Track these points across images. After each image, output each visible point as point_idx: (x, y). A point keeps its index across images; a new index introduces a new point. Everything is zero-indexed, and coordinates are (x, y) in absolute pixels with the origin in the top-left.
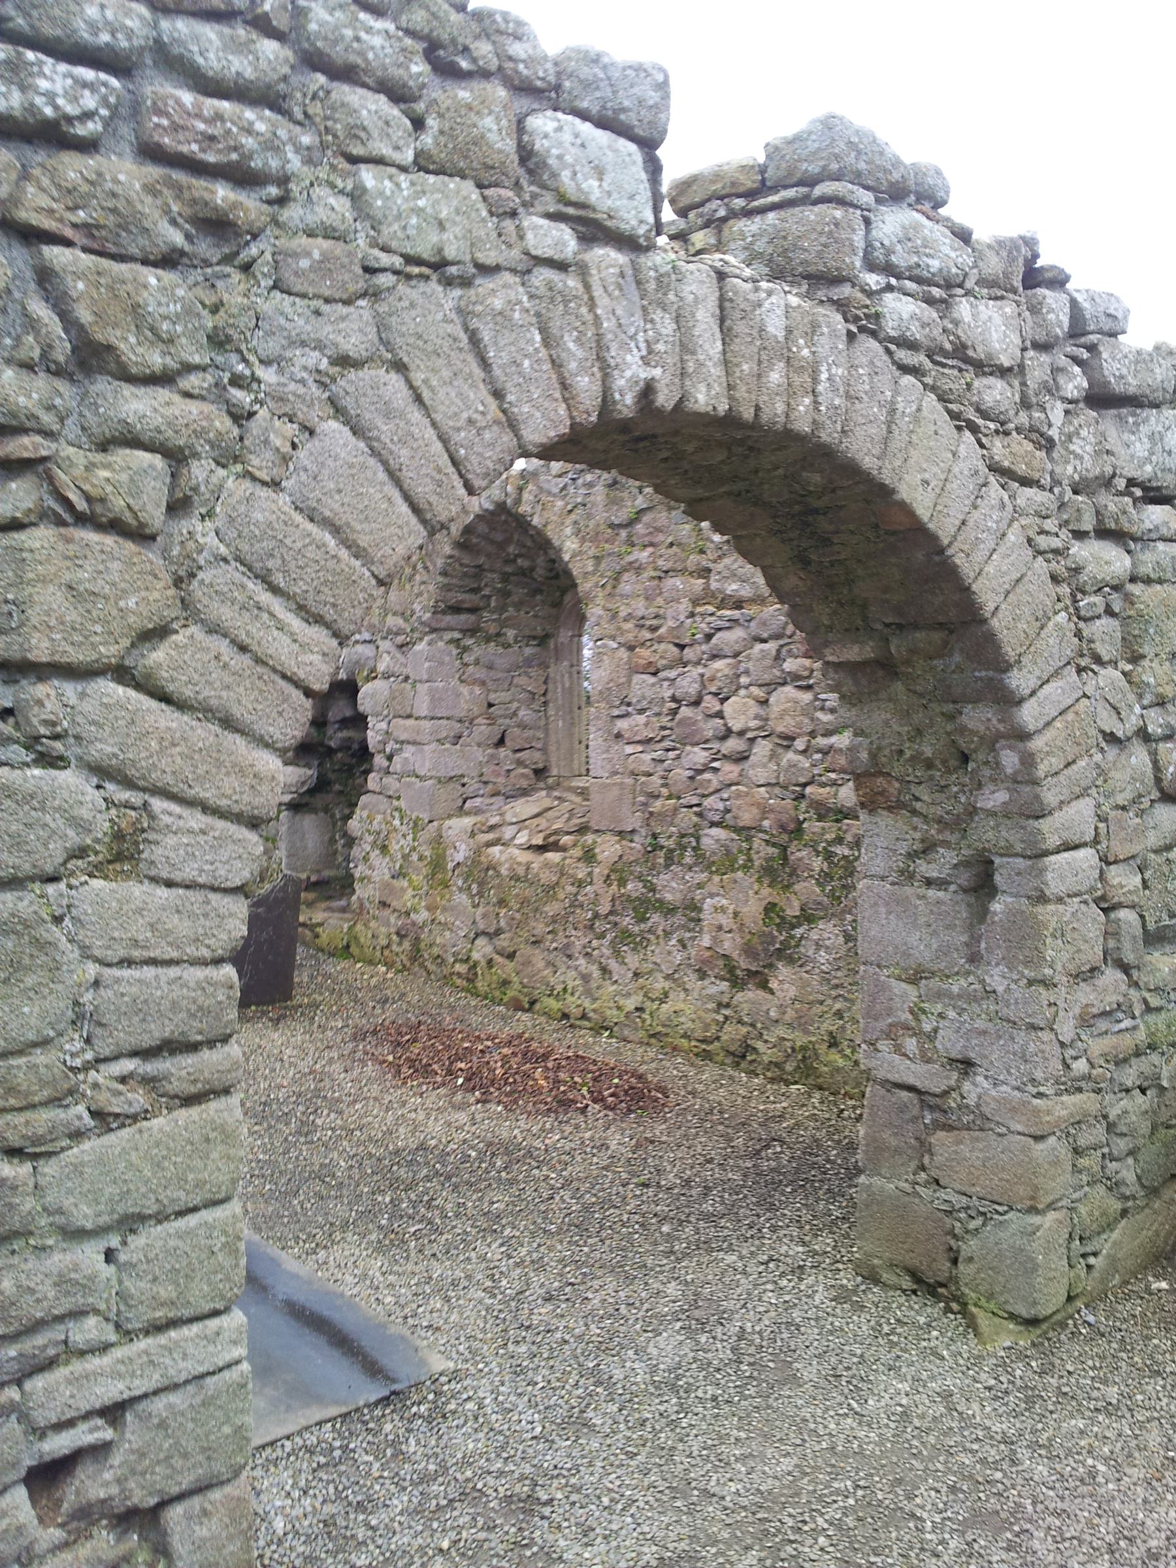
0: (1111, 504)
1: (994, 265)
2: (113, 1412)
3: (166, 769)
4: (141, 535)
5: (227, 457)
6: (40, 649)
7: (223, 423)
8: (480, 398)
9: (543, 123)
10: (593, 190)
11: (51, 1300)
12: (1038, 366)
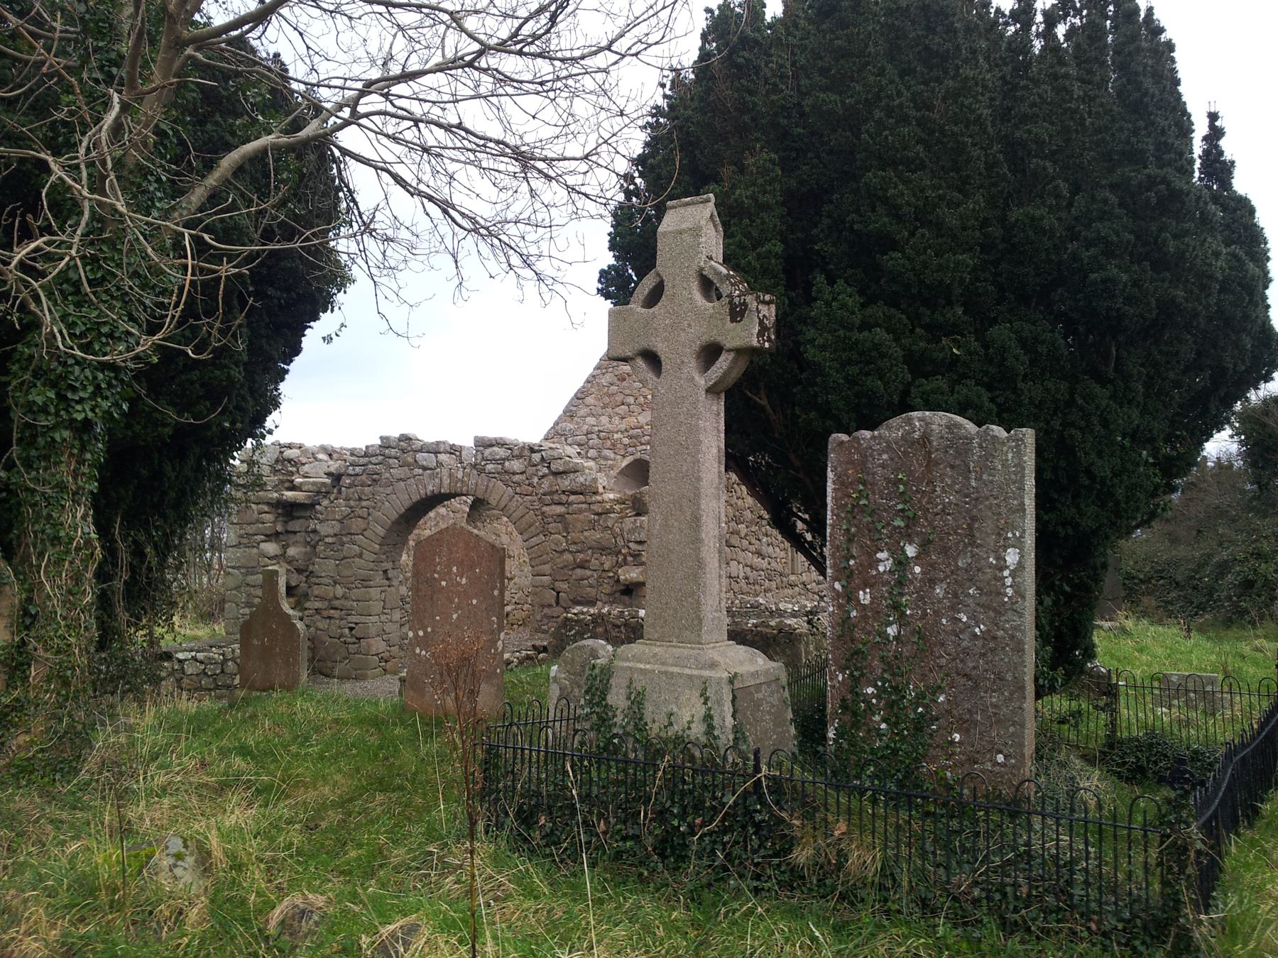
0: (556, 497)
1: (516, 452)
2: (356, 624)
3: (365, 546)
5: (374, 508)
7: (373, 504)
9: (419, 456)
10: (425, 463)
11: (349, 607)
12: (531, 470)
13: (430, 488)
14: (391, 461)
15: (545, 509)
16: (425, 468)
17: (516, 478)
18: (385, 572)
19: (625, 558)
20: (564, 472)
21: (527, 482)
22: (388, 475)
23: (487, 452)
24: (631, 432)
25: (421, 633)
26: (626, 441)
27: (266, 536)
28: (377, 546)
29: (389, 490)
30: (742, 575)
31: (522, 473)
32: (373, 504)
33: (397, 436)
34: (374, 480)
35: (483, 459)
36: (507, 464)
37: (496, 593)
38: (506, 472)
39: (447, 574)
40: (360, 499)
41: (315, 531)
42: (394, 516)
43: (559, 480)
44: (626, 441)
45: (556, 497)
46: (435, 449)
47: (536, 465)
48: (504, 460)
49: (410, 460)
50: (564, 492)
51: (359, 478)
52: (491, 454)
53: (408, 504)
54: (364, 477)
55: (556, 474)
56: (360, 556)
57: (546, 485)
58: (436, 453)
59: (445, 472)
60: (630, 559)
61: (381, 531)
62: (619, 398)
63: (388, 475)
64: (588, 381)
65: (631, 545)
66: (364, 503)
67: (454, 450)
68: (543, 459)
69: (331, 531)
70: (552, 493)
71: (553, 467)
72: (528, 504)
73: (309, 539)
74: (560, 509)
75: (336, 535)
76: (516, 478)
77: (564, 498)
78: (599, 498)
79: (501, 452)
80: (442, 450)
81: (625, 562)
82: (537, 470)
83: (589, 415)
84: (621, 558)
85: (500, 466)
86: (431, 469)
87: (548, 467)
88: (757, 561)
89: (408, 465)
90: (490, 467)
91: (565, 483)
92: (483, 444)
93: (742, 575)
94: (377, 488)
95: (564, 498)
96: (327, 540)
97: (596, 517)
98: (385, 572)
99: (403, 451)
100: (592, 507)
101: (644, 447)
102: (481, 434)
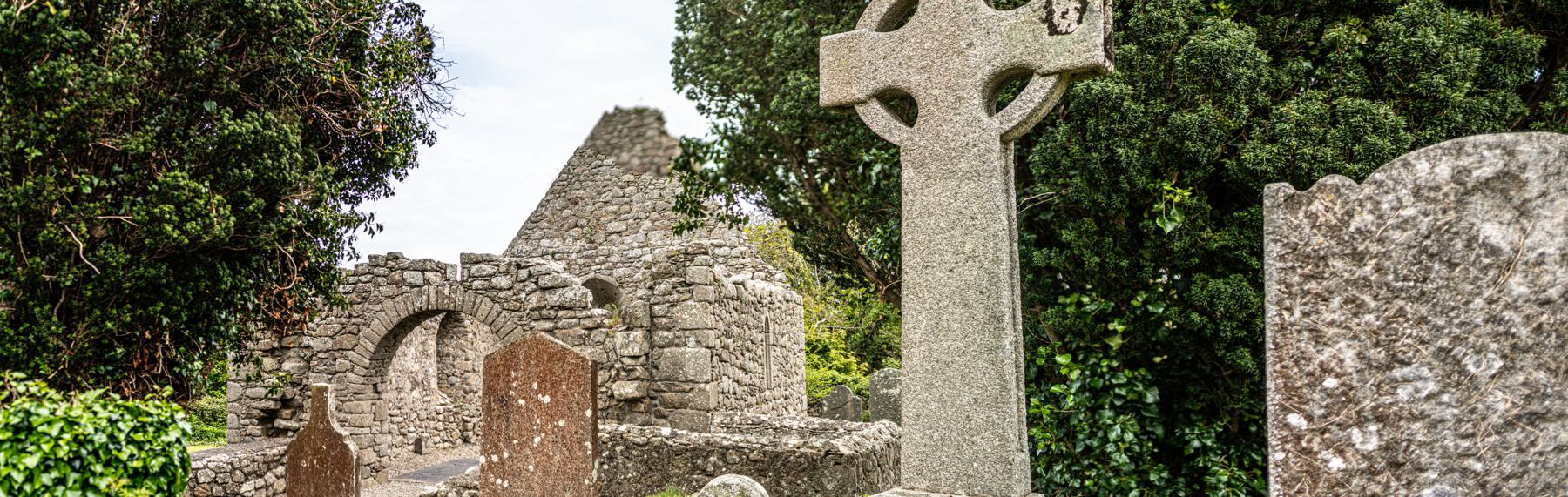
0: (544, 312)
3: (356, 361)
4: (353, 334)
5: (364, 324)
6: (344, 347)
7: (363, 321)
8: (395, 313)
9: (406, 274)
10: (412, 280)
13: (418, 305)
14: (380, 279)
15: (533, 324)
16: (412, 286)
17: (503, 294)
18: (375, 386)
19: (618, 374)
20: (552, 288)
21: (514, 298)
22: (376, 293)
23: (474, 269)
24: (585, 253)
25: (495, 458)
26: (581, 261)
27: (264, 351)
28: (368, 362)
29: (378, 307)
30: (731, 390)
31: (509, 289)
32: (363, 321)
33: (385, 254)
34: (364, 298)
35: (469, 276)
36: (494, 280)
37: (589, 413)
38: (493, 288)
39: (525, 392)
40: (350, 316)
41: (308, 347)
42: (383, 332)
43: (547, 296)
44: (581, 261)
45: (544, 312)
46: (422, 266)
47: (523, 281)
48: (491, 276)
49: (397, 277)
50: (552, 307)
51: (349, 296)
52: (477, 270)
53: (396, 321)
54: (354, 295)
55: (544, 289)
56: (352, 371)
57: (534, 300)
58: (423, 271)
59: (432, 290)
60: (623, 374)
61: (371, 348)
62: (572, 221)
63: (376, 293)
64: (541, 205)
65: (624, 360)
66: (353, 320)
67: (440, 268)
68: (530, 275)
69: (322, 346)
70: (540, 309)
71: (541, 283)
72: (516, 320)
73: (302, 355)
74: (548, 325)
75: (328, 351)
76: (503, 294)
77: (552, 313)
78: (589, 313)
79: (488, 269)
80: (428, 267)
81: (618, 377)
82: (525, 286)
83: (543, 238)
84: (614, 372)
85: (487, 283)
86: (418, 286)
87: (536, 283)
88: (741, 375)
89: (396, 283)
90: (476, 284)
91: (554, 298)
92: (469, 260)
93: (731, 390)
94: (366, 305)
95: (552, 313)
96: (320, 355)
97: (587, 332)
98: (375, 386)
99: (392, 269)
100: (582, 322)
101: (599, 267)
102: (467, 251)
